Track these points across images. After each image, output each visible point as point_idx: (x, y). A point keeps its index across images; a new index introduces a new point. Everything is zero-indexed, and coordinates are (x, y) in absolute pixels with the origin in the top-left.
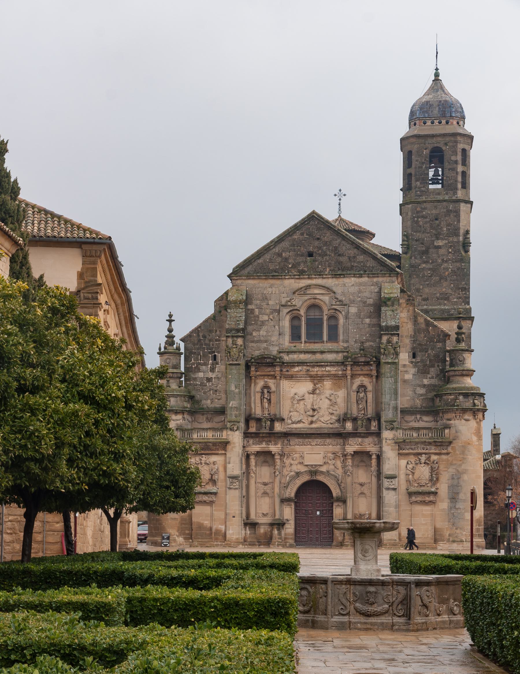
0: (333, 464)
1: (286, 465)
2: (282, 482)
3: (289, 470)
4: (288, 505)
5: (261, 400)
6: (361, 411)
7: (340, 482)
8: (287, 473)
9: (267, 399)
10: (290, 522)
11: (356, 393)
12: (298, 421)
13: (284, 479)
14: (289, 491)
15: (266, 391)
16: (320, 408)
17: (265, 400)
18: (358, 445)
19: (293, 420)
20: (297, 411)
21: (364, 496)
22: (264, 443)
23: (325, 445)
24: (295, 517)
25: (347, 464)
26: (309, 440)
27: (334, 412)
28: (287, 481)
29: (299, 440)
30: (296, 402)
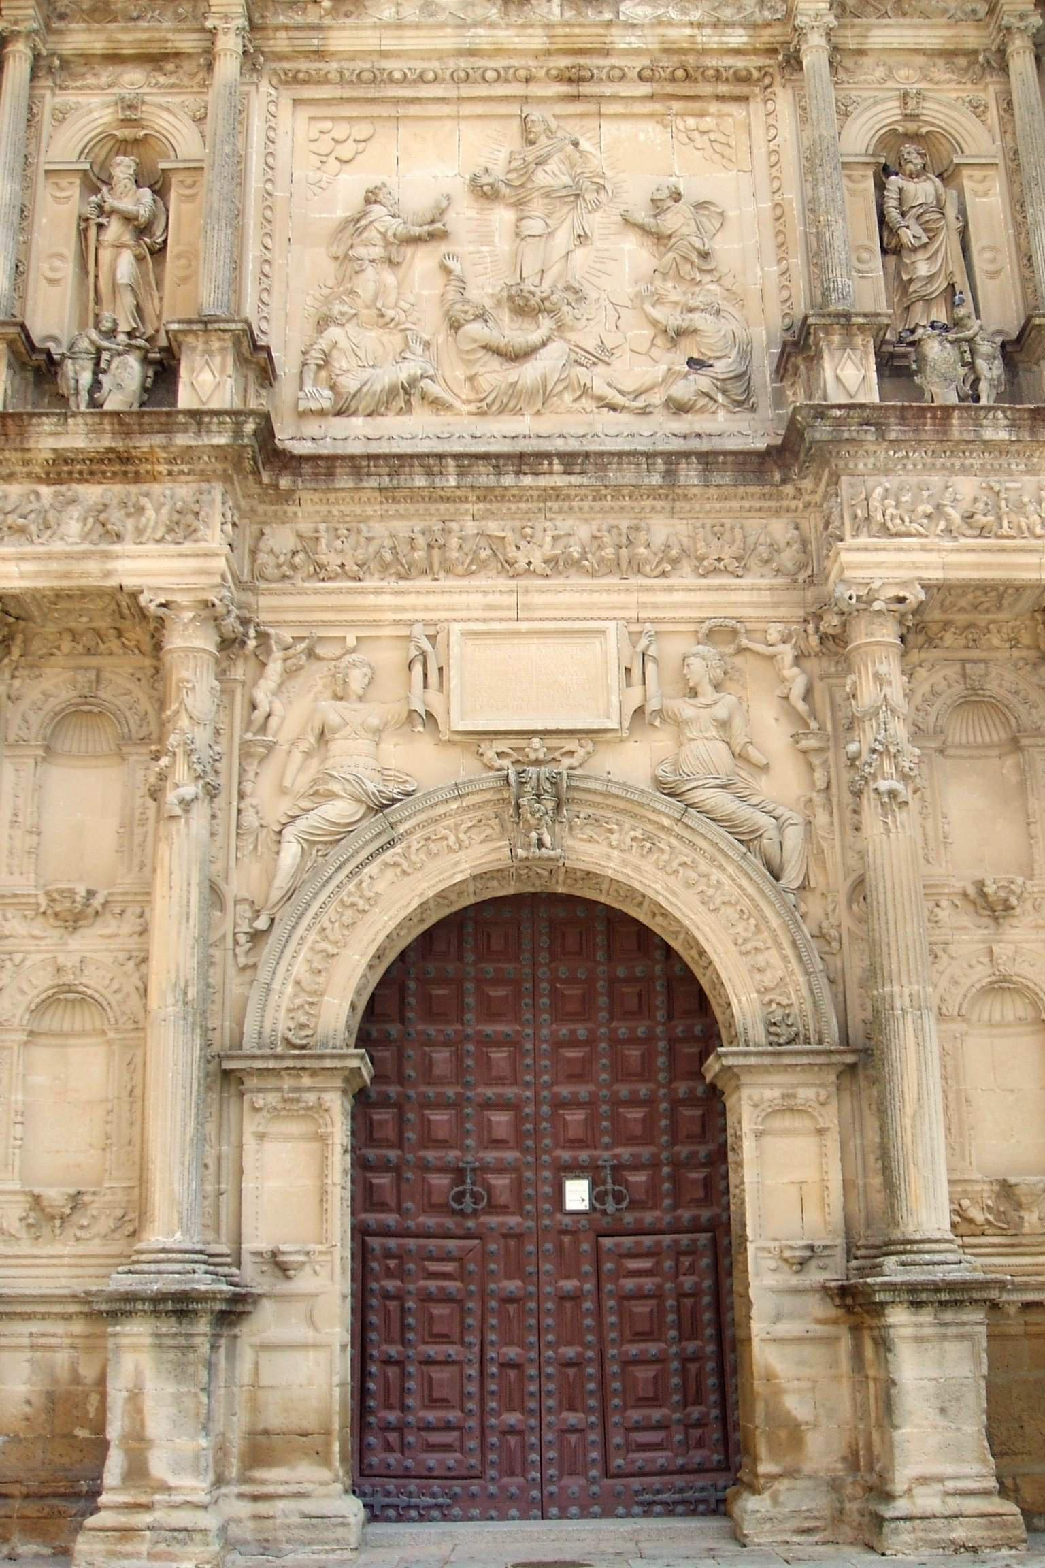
0: (724, 725)
1: (284, 737)
2: (234, 888)
3: (302, 782)
4: (290, 1108)
5: (83, 234)
6: (928, 301)
7: (792, 878)
8: (285, 806)
9: (128, 219)
10: (303, 1282)
11: (870, 184)
12: (392, 392)
13: (256, 869)
14: (300, 969)
15: (123, 168)
16: (576, 294)
17: (115, 229)
18: (948, 531)
19: (350, 384)
20: (383, 320)
21: (1014, 1009)
22: (73, 527)
23: (636, 567)
24: (360, 1233)
25: (868, 694)
26: (493, 527)
27: (699, 321)
28: (282, 881)
29: (402, 528)
30: (377, 252)
